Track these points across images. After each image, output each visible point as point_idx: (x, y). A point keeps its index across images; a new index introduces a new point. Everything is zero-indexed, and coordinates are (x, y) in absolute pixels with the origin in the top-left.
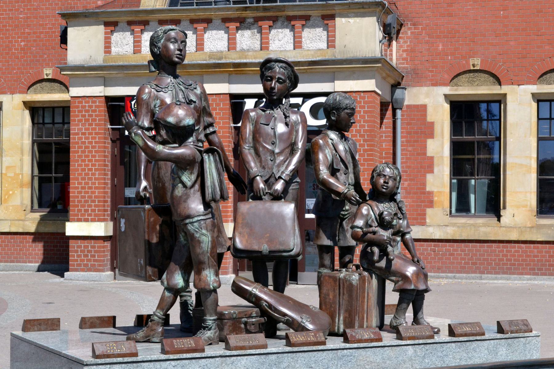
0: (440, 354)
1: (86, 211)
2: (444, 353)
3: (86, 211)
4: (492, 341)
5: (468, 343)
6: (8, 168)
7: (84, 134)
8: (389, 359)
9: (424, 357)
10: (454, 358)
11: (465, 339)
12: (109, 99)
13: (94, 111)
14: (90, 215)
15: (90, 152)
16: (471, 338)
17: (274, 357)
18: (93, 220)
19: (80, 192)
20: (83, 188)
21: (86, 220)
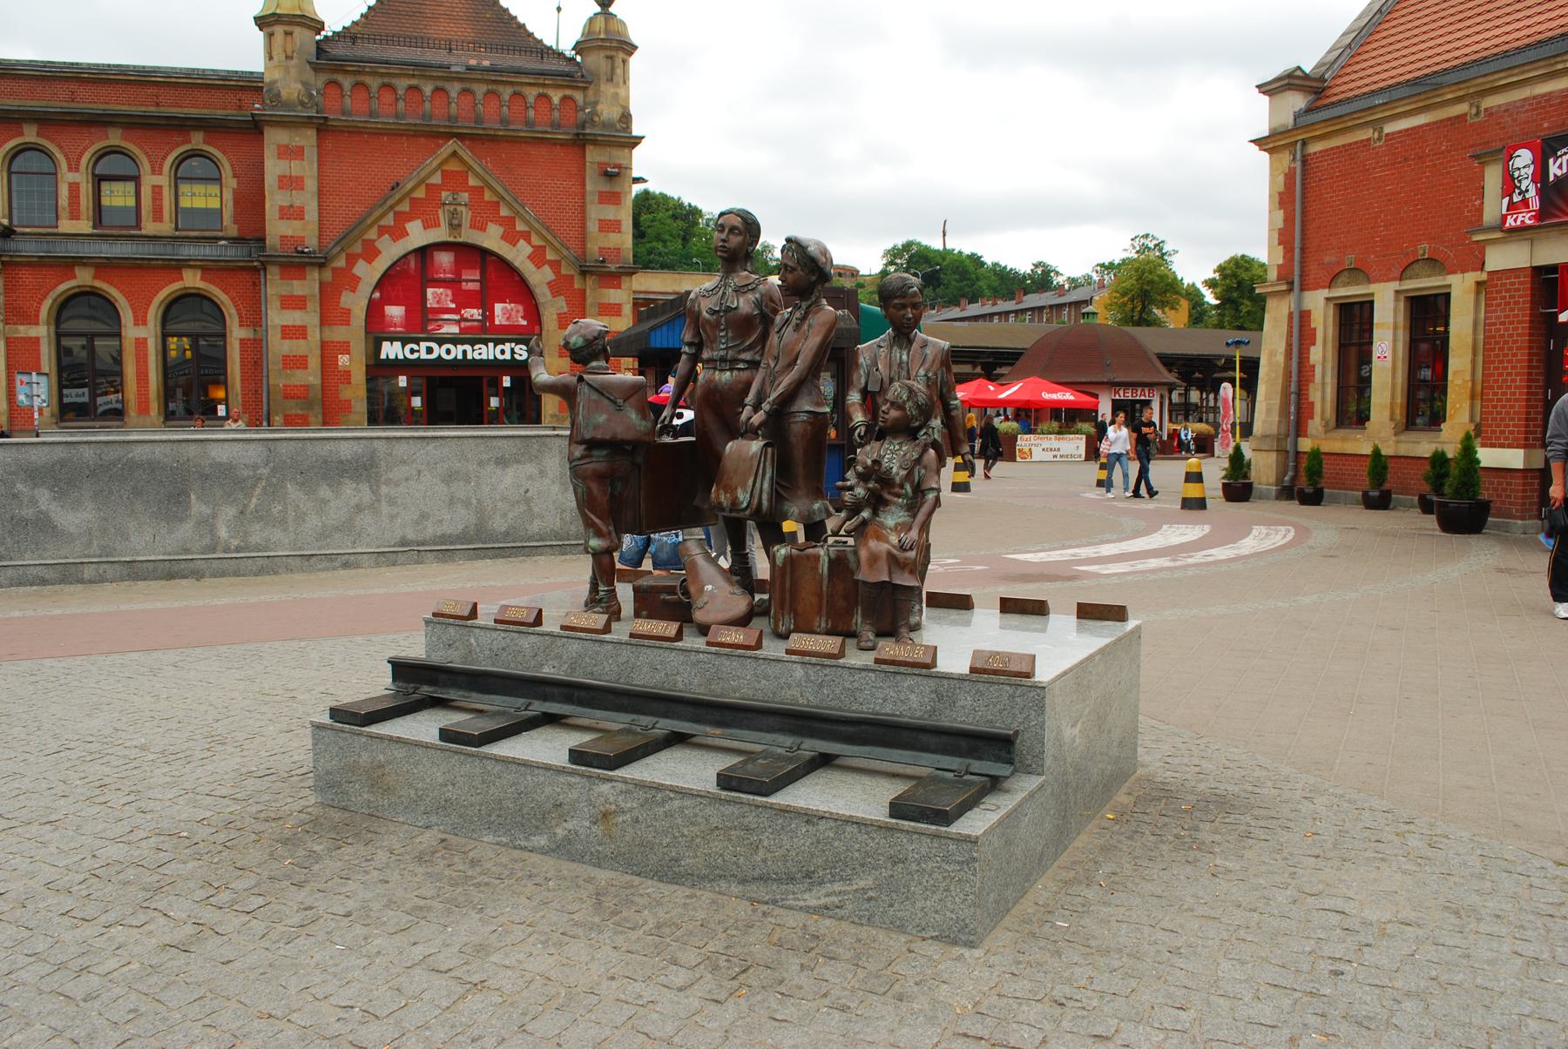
0: (848, 685)
1: (1502, 432)
2: (856, 685)
3: (1502, 432)
4: (945, 682)
5: (899, 678)
6: (1455, 373)
7: (1503, 323)
8: (766, 677)
9: (821, 686)
10: (872, 695)
11: (892, 668)
12: (1537, 271)
13: (1517, 290)
14: (1506, 439)
15: (1510, 349)
16: (902, 669)
17: (610, 647)
18: (1510, 446)
19: (1495, 407)
20: (1499, 400)
21: (1502, 446)
